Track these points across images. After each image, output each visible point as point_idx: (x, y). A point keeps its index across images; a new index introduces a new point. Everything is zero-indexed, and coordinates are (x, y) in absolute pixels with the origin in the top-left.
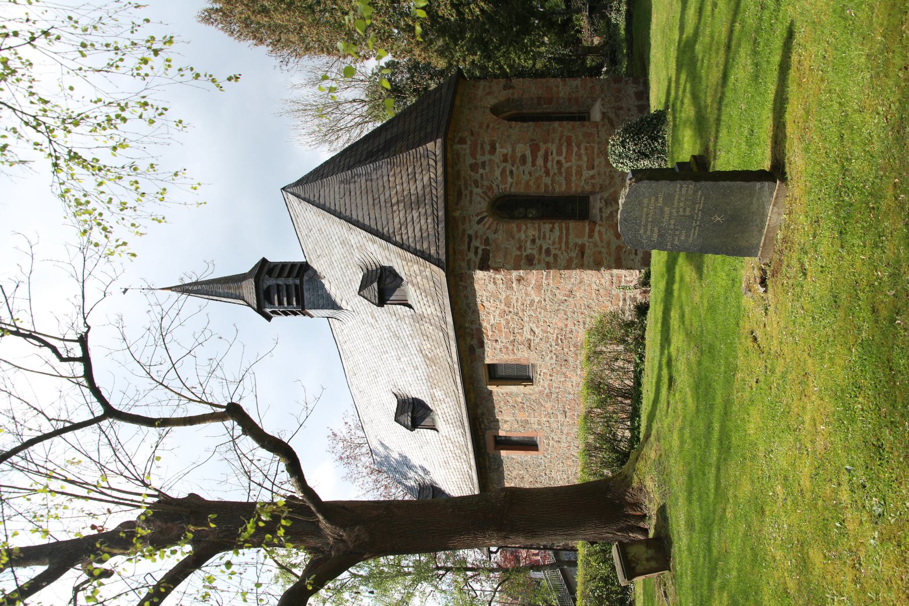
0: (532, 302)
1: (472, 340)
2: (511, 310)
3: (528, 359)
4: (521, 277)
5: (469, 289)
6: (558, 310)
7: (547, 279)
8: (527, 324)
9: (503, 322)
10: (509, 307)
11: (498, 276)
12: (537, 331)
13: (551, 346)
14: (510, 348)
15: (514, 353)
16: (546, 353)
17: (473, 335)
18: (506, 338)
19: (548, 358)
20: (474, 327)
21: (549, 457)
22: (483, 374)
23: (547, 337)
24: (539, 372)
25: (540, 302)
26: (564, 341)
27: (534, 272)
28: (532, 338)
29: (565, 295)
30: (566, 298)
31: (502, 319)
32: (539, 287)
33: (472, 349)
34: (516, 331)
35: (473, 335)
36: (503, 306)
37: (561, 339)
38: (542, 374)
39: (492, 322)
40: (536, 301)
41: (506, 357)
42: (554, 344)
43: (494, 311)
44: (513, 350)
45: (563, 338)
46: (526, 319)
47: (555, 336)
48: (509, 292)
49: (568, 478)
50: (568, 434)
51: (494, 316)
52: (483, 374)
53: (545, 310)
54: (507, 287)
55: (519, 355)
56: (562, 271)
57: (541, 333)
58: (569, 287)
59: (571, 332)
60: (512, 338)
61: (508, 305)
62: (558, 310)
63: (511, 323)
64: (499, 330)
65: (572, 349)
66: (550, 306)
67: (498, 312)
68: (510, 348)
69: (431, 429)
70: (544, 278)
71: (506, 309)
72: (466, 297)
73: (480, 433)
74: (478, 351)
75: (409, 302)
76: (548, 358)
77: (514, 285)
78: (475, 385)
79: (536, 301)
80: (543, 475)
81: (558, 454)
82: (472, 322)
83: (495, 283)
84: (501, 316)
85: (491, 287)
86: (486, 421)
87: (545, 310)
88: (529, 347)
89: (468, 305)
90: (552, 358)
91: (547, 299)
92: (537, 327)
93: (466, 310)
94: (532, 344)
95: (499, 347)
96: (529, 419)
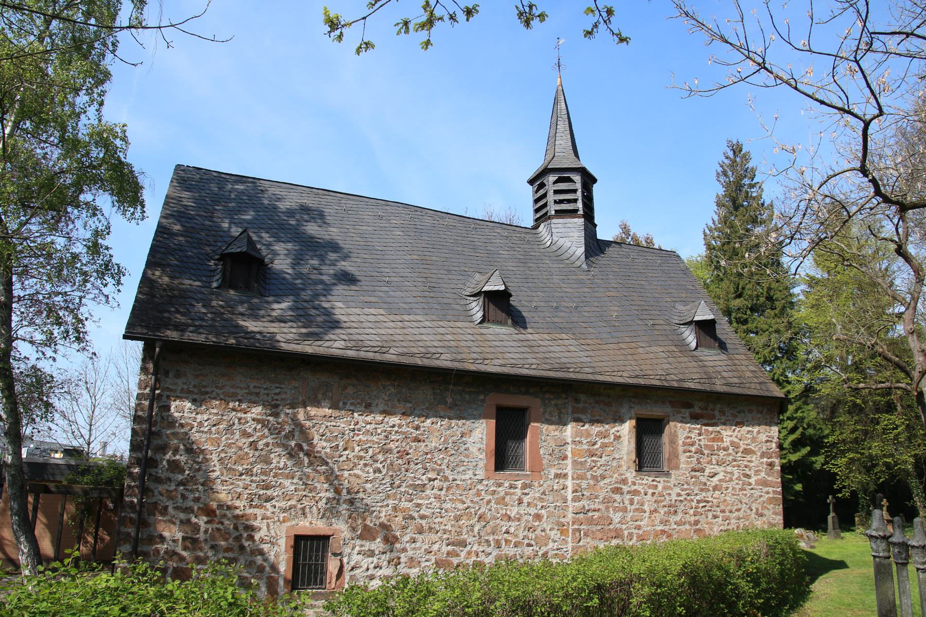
0: (748, 476)
1: (700, 407)
2: (739, 454)
3: (677, 468)
4: (774, 466)
5: (759, 415)
6: (741, 502)
7: (774, 492)
8: (723, 469)
9: (725, 445)
10: (742, 452)
11: (774, 445)
12: (715, 479)
13: (696, 494)
14: (693, 449)
15: (685, 452)
16: (686, 489)
17: (706, 409)
18: (706, 446)
19: (678, 490)
20: (717, 413)
21: (480, 487)
22: (653, 411)
23: (709, 490)
24: (658, 479)
25: (750, 484)
26: (703, 509)
27: (779, 480)
28: (706, 474)
29: (757, 510)
30: (754, 510)
31: (728, 444)
32: (764, 483)
33: (688, 406)
34: (714, 457)
35: (706, 409)
36: (743, 447)
37: (705, 506)
38: (655, 483)
39: (724, 433)
40: (750, 481)
41: (680, 442)
42: (698, 498)
43: (736, 437)
44: (690, 451)
45: (707, 508)
46: (729, 469)
47: (710, 499)
48: (759, 454)
49: (423, 517)
50: (538, 517)
51: (731, 436)
52: (653, 411)
53: (741, 489)
54: (763, 452)
55: (683, 458)
56: (781, 506)
57: (713, 484)
58: (766, 512)
59: (715, 517)
60: (706, 452)
61: (747, 452)
62: (741, 502)
63: (725, 453)
64: (714, 438)
65: (693, 519)
66: (746, 495)
67: (736, 440)
68: (693, 449)
69: (484, 316)
70: (775, 489)
71: (741, 450)
72: (750, 411)
73: (531, 391)
74: (686, 412)
75: (699, 348)
76: (678, 490)
77: (765, 460)
78: (633, 400)
79: (750, 481)
80: (432, 475)
81: (489, 502)
82: (722, 413)
83: (767, 441)
84: (732, 443)
85: (763, 437)
86: (559, 402)
87: (741, 489)
88: (694, 470)
89: (744, 412)
90: (679, 495)
91: (752, 491)
92: (720, 480)
93: (736, 408)
94: (698, 474)
95: (693, 437)
96: (569, 461)
